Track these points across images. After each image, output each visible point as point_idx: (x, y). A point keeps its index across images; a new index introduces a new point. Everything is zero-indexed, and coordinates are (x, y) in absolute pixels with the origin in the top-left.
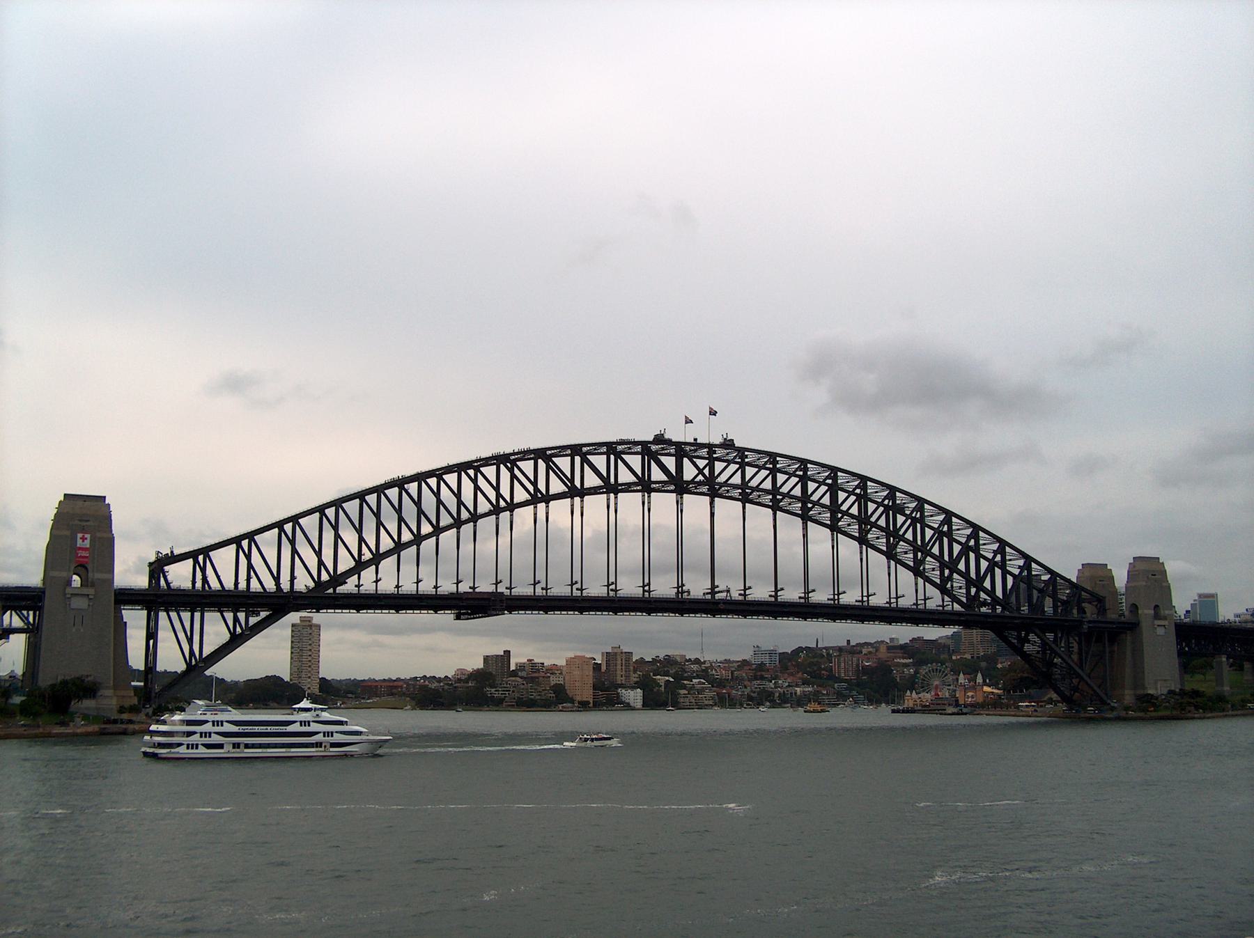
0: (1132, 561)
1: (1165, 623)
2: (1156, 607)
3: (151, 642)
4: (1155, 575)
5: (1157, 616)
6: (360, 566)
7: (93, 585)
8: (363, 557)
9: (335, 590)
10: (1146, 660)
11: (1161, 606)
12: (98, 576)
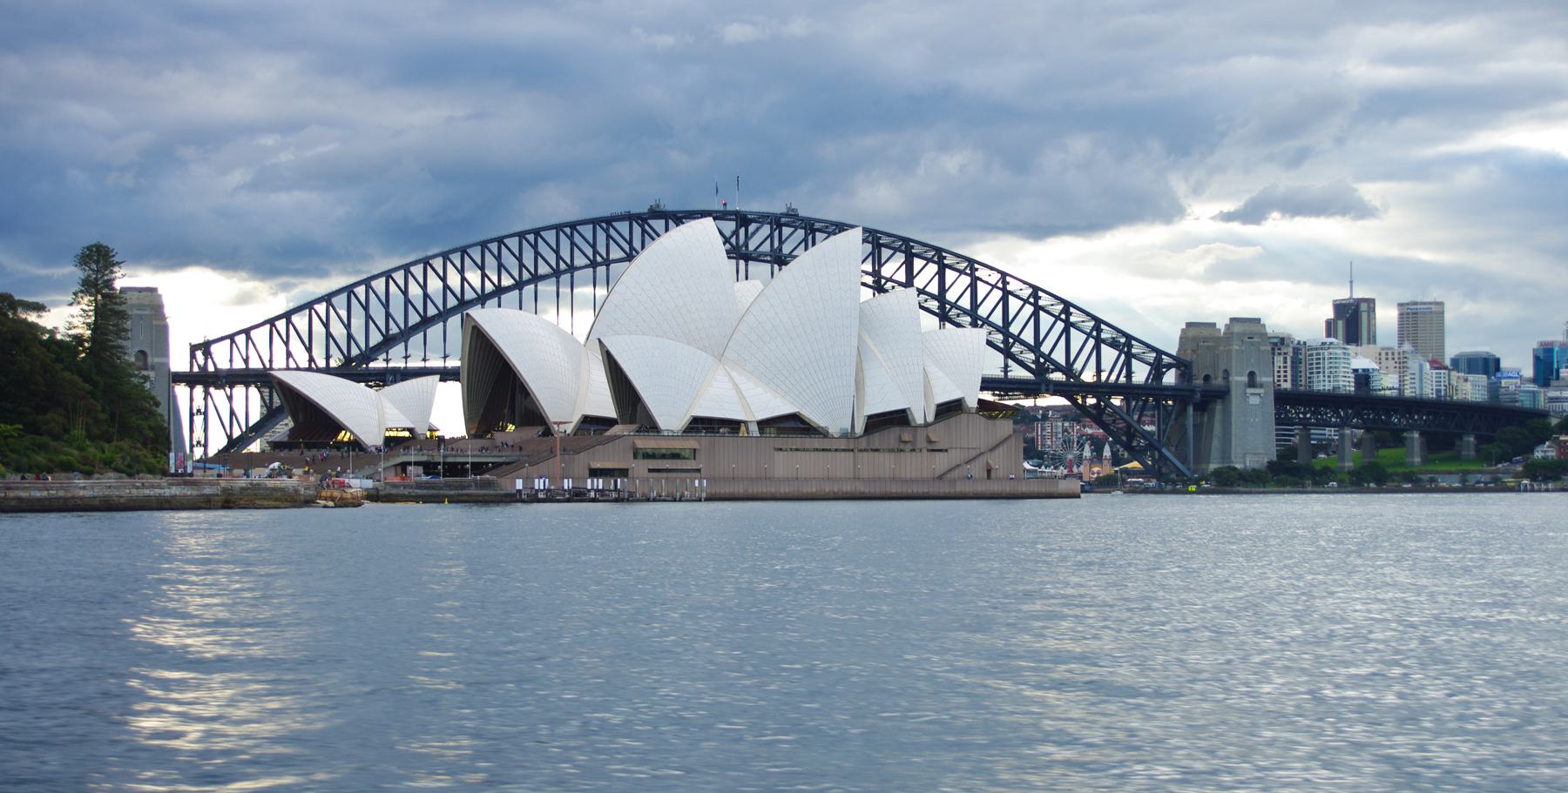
0: (1228, 323)
1: (1261, 391)
2: (1252, 374)
3: (199, 420)
4: (1252, 338)
5: (1252, 383)
6: (388, 341)
7: (153, 368)
8: (391, 332)
9: (367, 365)
10: (1233, 432)
11: (1257, 373)
12: (157, 360)
